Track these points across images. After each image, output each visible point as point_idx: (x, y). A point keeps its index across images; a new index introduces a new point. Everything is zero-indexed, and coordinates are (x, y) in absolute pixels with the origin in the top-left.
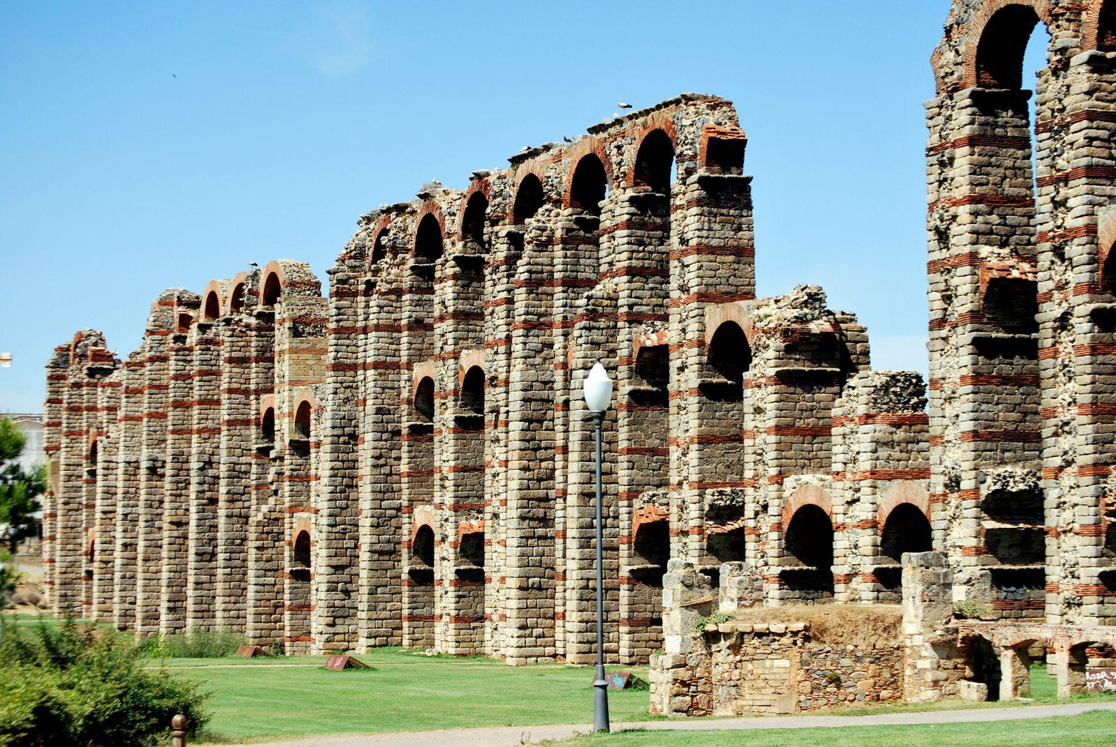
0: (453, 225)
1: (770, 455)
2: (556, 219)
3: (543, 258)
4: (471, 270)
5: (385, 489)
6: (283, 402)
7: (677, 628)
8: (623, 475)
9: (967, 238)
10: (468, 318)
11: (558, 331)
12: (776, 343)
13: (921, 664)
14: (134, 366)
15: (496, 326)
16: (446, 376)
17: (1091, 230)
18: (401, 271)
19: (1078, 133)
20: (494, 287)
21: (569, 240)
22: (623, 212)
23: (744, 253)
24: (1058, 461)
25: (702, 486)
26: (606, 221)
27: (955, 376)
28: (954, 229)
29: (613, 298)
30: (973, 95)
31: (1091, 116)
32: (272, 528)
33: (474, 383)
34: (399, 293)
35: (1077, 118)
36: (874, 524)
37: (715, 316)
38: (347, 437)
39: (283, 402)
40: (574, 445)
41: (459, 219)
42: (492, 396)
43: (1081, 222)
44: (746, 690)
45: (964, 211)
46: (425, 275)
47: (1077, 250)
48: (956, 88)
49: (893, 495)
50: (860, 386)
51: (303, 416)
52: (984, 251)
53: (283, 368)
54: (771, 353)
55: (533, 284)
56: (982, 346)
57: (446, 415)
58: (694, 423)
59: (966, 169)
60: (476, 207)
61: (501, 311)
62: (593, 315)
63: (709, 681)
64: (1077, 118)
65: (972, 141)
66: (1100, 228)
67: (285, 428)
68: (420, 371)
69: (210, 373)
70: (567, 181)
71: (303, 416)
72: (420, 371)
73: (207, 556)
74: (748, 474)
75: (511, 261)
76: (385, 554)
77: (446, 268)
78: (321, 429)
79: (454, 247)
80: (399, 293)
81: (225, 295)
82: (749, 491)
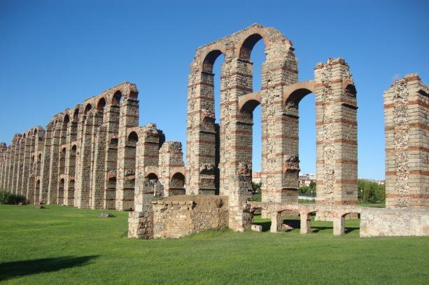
0: (72, 116)
1: (142, 162)
2: (94, 111)
3: (90, 120)
4: (75, 125)
5: (55, 170)
6: (36, 154)
7: (141, 202)
8: (106, 167)
9: (199, 107)
10: (74, 135)
11: (93, 136)
12: (145, 135)
13: (237, 218)
14: (9, 148)
15: (79, 136)
16: (68, 147)
17: (237, 102)
18: (59, 126)
19: (234, 78)
20: (80, 127)
21: (96, 116)
22: (109, 109)
23: (136, 117)
24: (225, 161)
25: (125, 169)
26: (105, 111)
27: (194, 140)
28: (195, 105)
29: (106, 128)
30: (202, 73)
31: (237, 73)
32: (33, 178)
33: (74, 148)
34: (60, 130)
35: (234, 74)
36: (169, 177)
37: (130, 130)
38: (47, 160)
39: (36, 154)
40: (95, 160)
41: (73, 114)
42: (78, 150)
43: (234, 100)
44: (168, 227)
45: (198, 100)
46: (65, 126)
47: (233, 107)
48: (198, 71)
49: (175, 171)
50: (166, 147)
51: (40, 156)
52: (203, 110)
53: (36, 147)
54: (144, 138)
55: (88, 125)
56: (202, 132)
57: (68, 154)
58: (123, 155)
59: (199, 90)
60: (77, 112)
61: (81, 132)
62: (101, 131)
63: (152, 223)
64: (234, 74)
65: (201, 83)
66: (239, 101)
67: (36, 159)
68: (63, 146)
69: (23, 149)
70: (97, 104)
71: (40, 156)
72: (63, 146)
73: (20, 184)
74: (137, 166)
75: (83, 122)
76: (54, 183)
77: (70, 124)
78: (43, 158)
79: (71, 120)
80: (60, 130)
81: (27, 134)
82: (137, 170)
